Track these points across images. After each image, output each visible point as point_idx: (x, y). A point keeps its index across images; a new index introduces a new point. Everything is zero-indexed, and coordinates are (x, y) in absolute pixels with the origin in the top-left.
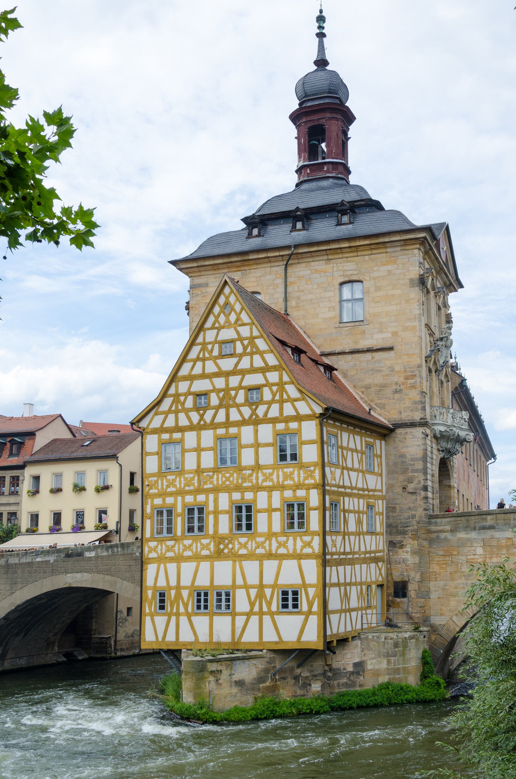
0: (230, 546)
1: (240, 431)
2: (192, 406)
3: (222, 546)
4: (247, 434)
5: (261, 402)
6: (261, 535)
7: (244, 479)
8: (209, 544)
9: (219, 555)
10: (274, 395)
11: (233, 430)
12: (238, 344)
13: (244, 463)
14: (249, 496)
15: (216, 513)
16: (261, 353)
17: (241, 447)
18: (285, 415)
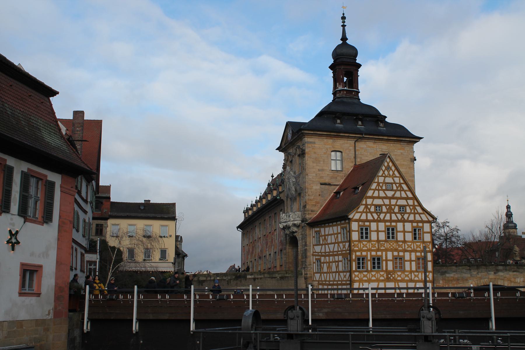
0: (393, 276)
1: (396, 224)
2: (373, 211)
3: (390, 276)
4: (400, 226)
5: (406, 213)
6: (407, 271)
7: (399, 246)
8: (384, 275)
9: (388, 280)
10: (411, 210)
11: (394, 224)
12: (394, 185)
13: (399, 239)
14: (401, 254)
15: (387, 260)
16: (405, 191)
17: (397, 232)
18: (417, 219)
